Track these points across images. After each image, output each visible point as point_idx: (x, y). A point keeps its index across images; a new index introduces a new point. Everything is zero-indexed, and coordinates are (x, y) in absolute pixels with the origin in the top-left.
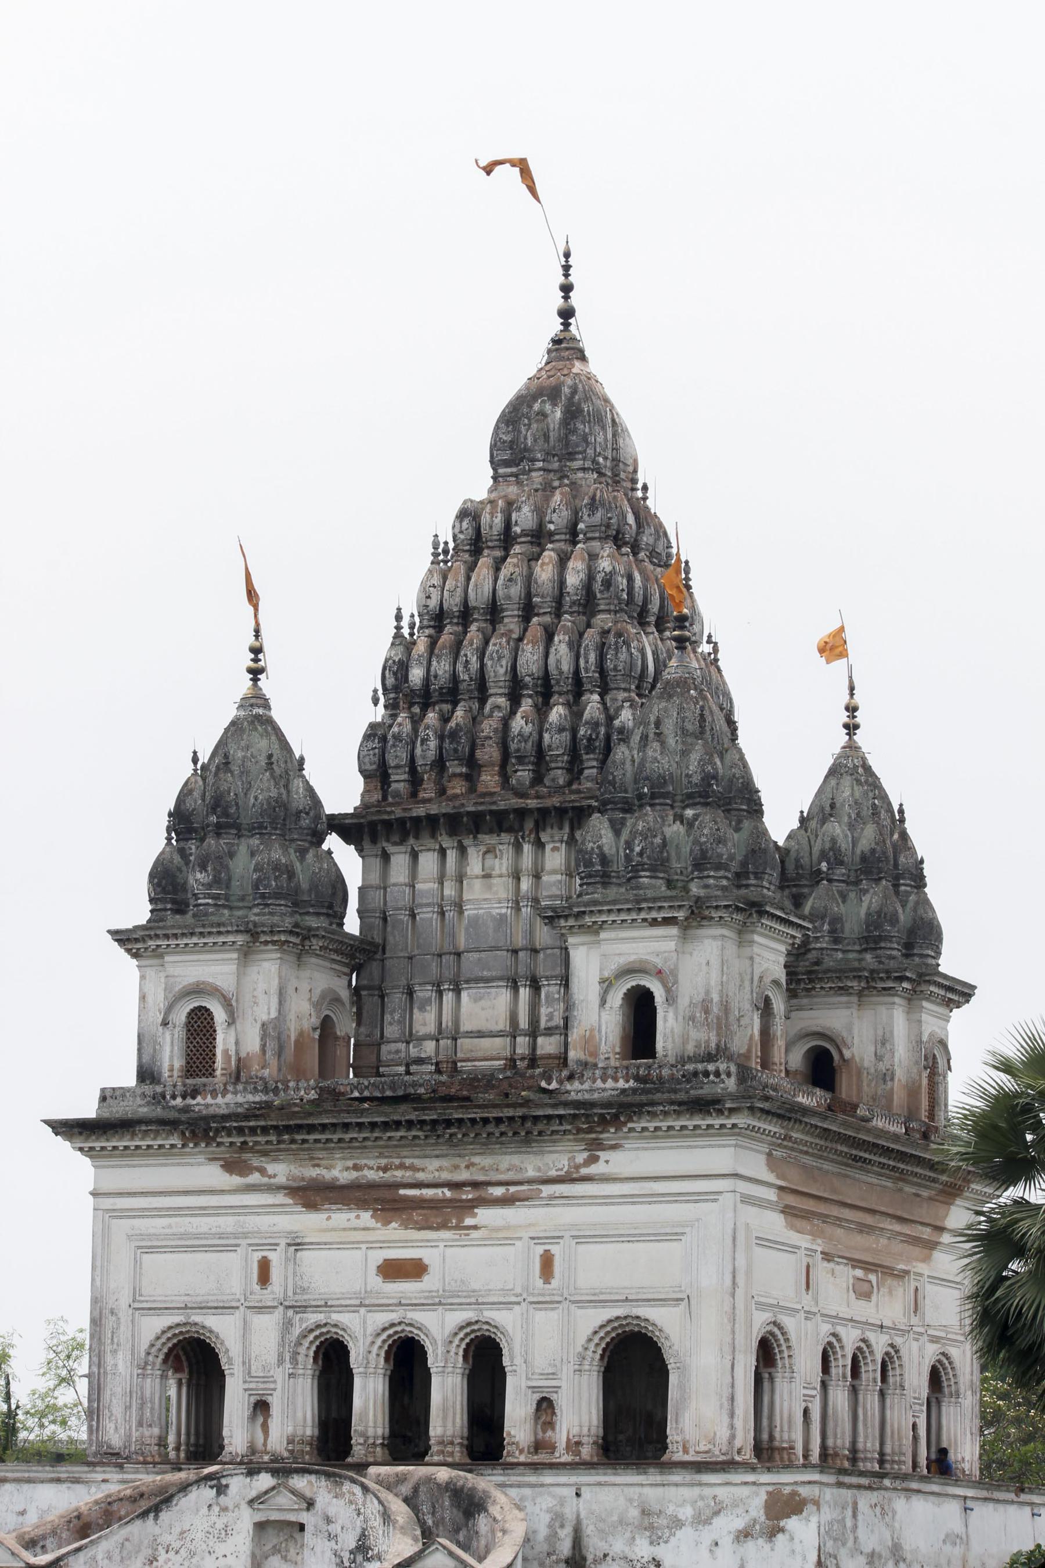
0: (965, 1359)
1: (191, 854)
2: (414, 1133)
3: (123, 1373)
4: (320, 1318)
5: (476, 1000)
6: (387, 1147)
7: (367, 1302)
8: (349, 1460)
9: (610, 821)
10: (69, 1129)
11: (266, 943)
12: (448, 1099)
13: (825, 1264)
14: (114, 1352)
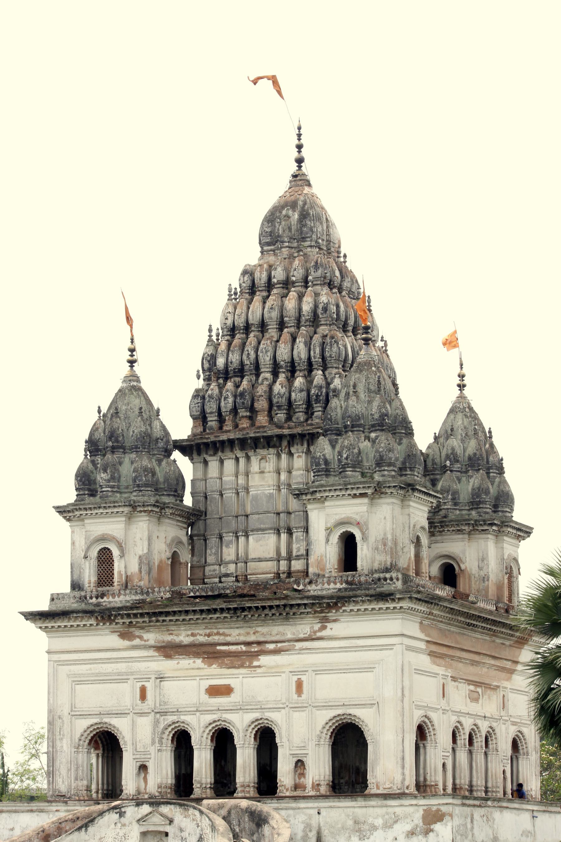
0: (531, 734)
1: (98, 463)
2: (224, 615)
3: (66, 751)
4: (175, 718)
5: (257, 541)
6: (210, 623)
7: (200, 709)
8: (192, 796)
9: (330, 440)
11: (141, 511)
12: (242, 596)
13: (453, 683)
14: (61, 739)
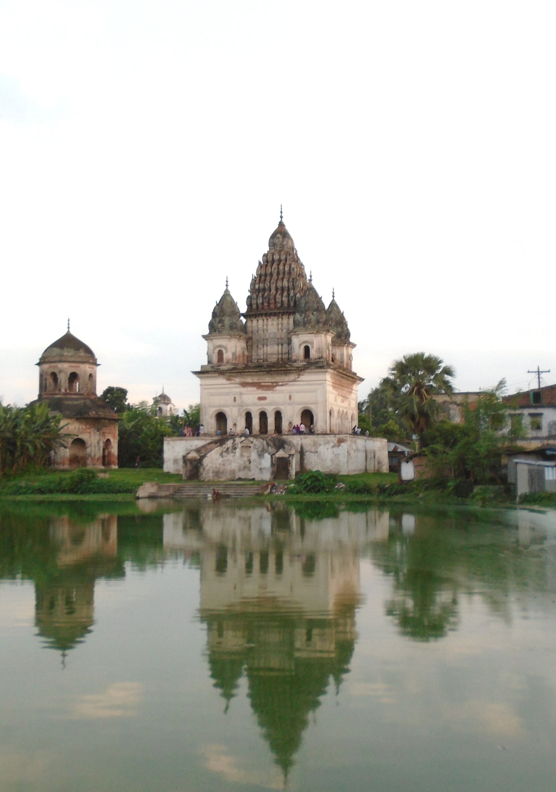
10: (196, 373)
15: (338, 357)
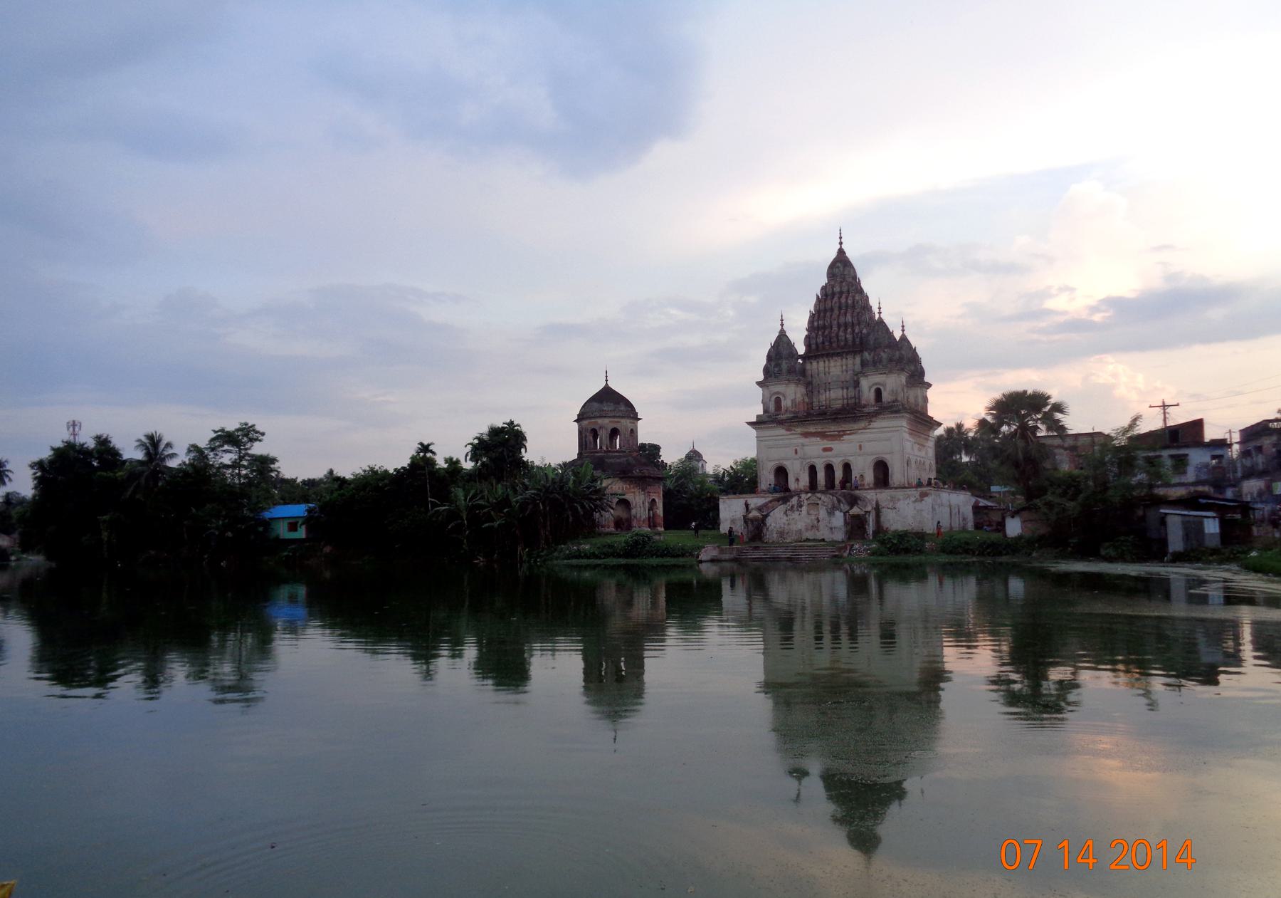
10: (750, 424)
15: (912, 400)
